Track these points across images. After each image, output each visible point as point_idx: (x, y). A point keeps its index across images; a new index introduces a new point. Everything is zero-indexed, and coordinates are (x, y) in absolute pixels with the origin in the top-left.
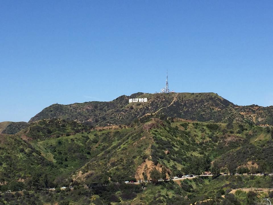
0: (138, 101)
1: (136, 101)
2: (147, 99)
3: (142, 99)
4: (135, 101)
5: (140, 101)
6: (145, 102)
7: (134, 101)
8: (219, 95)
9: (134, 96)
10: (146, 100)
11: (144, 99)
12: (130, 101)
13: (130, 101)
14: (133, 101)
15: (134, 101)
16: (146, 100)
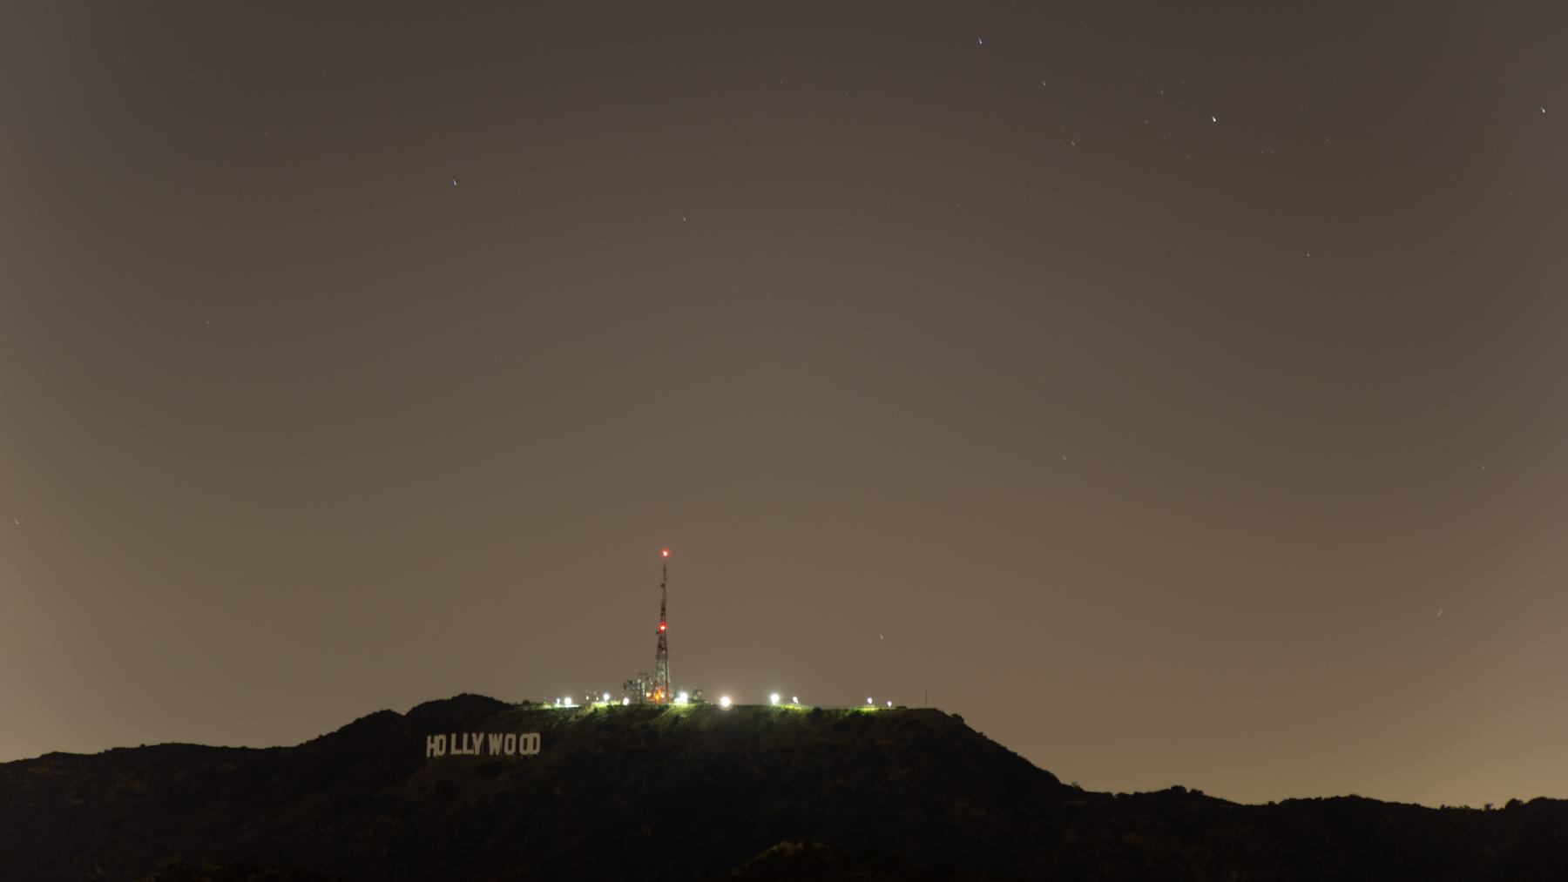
0: (486, 743)
1: (470, 746)
2: (538, 736)
3: (513, 736)
4: (466, 751)
5: (495, 744)
6: (525, 757)
7: (459, 746)
8: (974, 722)
9: (435, 716)
10: (531, 744)
11: (523, 736)
12: (435, 746)
13: (435, 746)
14: (454, 751)
15: (459, 746)
16: (531, 744)
